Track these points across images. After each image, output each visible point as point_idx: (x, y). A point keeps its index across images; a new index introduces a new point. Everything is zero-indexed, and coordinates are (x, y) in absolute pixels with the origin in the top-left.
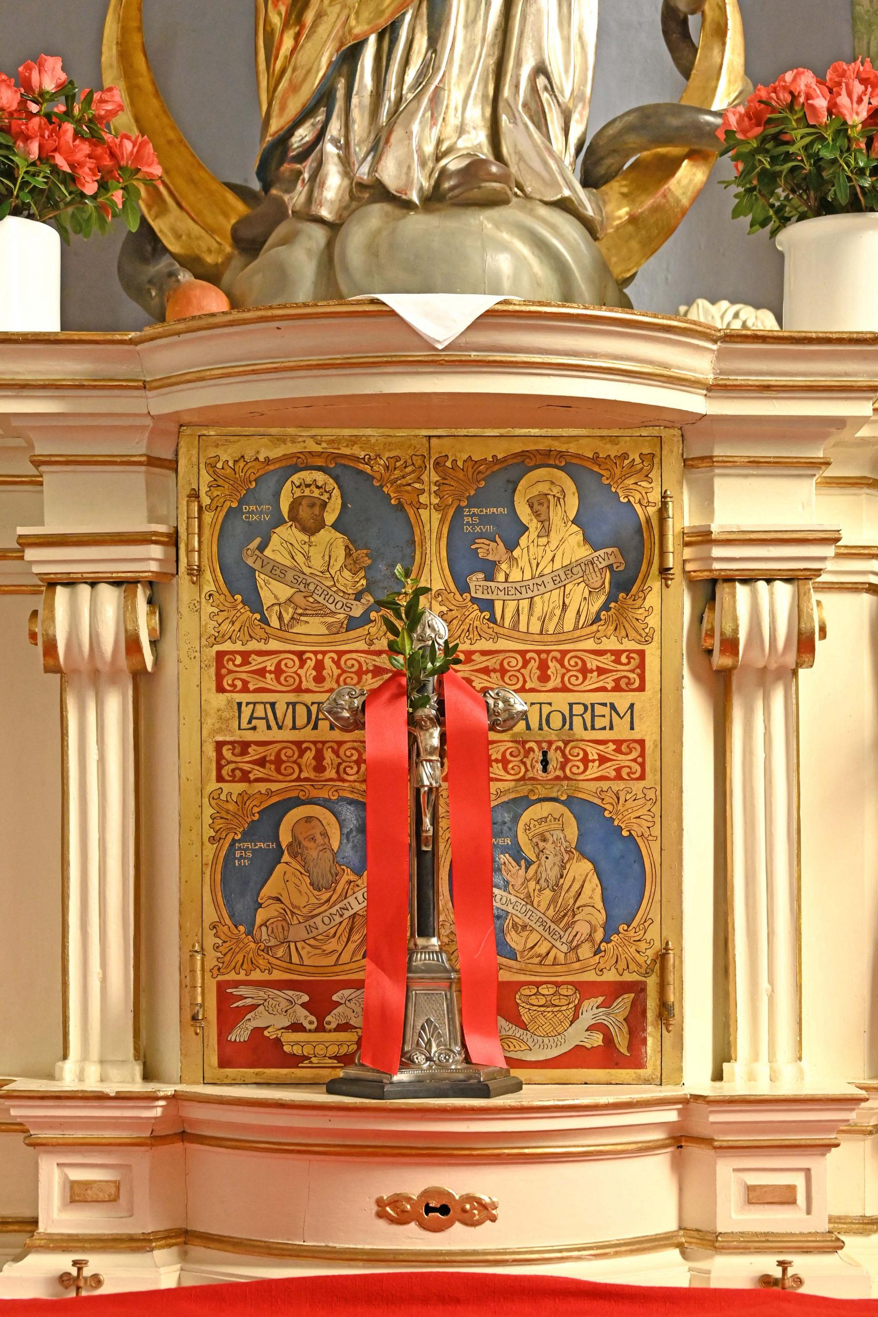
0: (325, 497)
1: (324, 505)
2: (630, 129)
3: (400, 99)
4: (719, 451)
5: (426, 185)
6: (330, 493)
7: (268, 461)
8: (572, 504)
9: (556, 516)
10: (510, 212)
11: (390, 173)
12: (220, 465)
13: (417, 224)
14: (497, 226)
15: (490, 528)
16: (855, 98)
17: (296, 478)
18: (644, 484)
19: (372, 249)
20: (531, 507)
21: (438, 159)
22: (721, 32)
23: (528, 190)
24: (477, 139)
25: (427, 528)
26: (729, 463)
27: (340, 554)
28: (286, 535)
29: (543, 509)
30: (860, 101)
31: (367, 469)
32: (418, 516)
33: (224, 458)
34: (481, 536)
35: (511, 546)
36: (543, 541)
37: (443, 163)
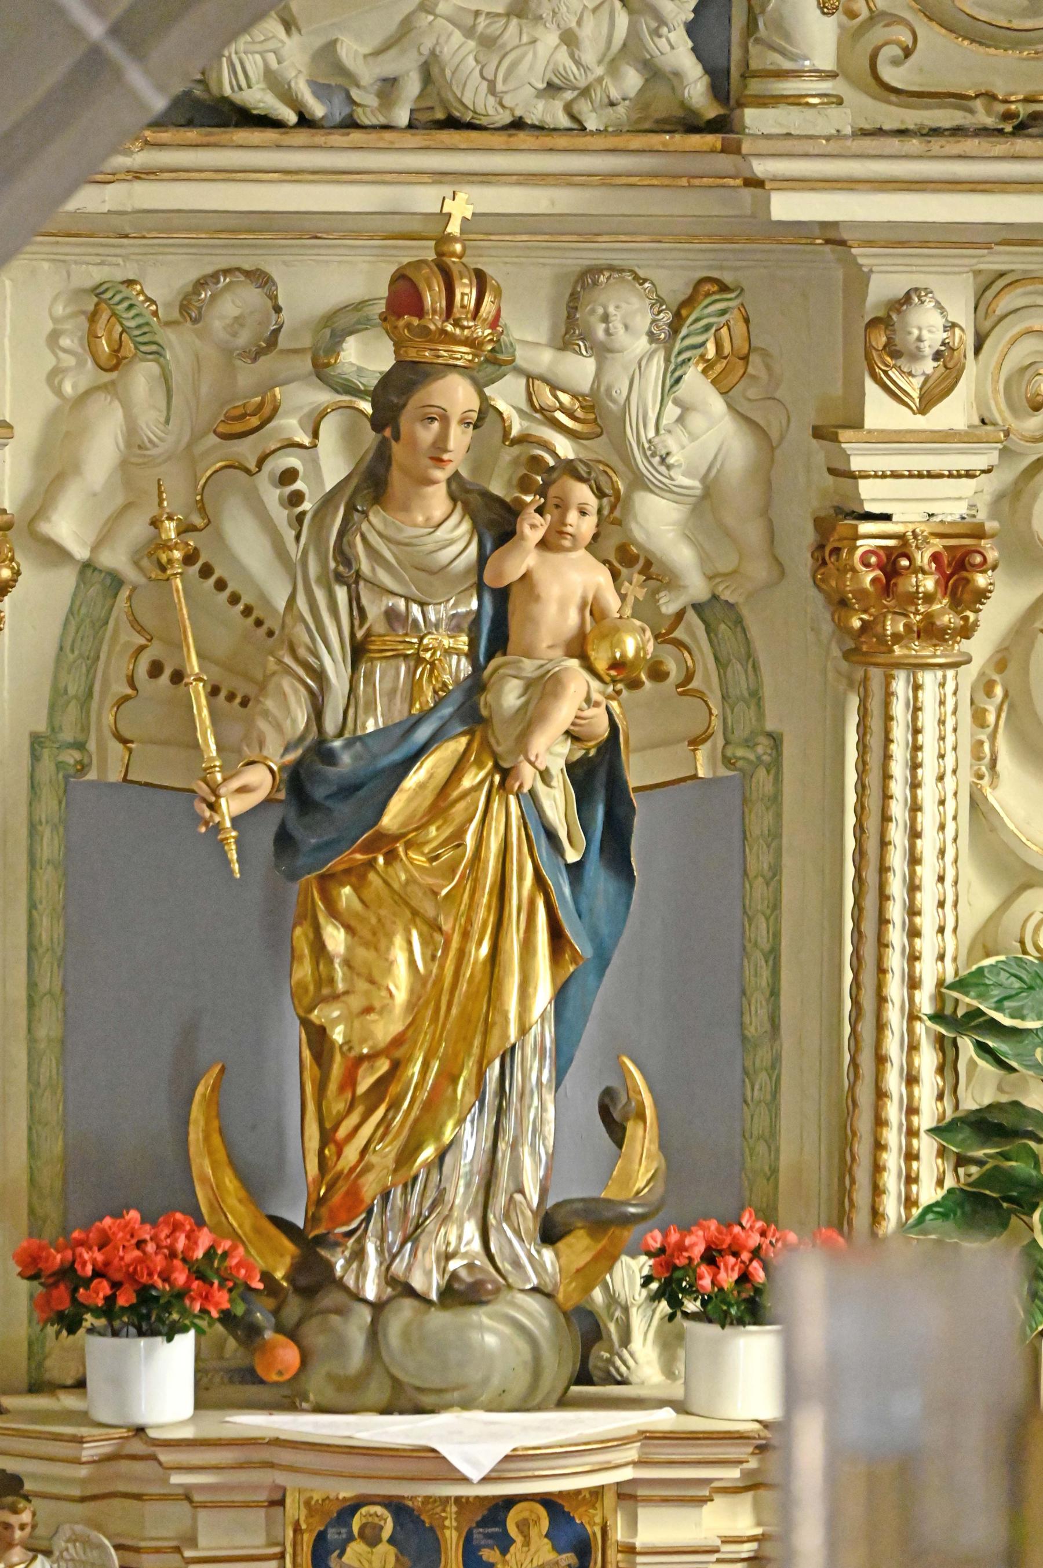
0: (382, 1523)
1: (381, 1528)
2: (576, 1213)
3: (420, 1214)
4: (641, 1492)
5: (441, 1282)
6: (385, 1520)
7: (344, 1499)
8: (545, 1524)
9: (534, 1532)
10: (500, 1307)
11: (417, 1282)
12: (313, 1502)
13: (439, 1319)
14: (490, 1317)
15: (490, 1542)
16: (730, 1267)
17: (364, 1510)
18: (591, 1511)
19: (406, 1335)
20: (518, 1526)
21: (449, 1257)
22: (641, 1116)
23: (510, 1280)
24: (477, 1246)
25: (449, 1542)
26: (649, 1501)
27: (392, 1560)
28: (356, 1549)
29: (525, 1529)
30: (733, 1269)
31: (410, 1504)
32: (444, 1535)
33: (315, 1499)
34: (484, 1546)
35: (504, 1551)
36: (525, 1549)
37: (454, 1265)
